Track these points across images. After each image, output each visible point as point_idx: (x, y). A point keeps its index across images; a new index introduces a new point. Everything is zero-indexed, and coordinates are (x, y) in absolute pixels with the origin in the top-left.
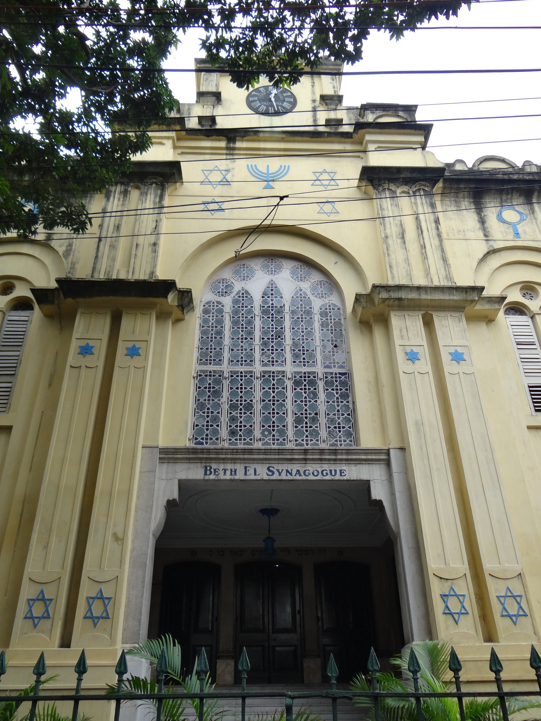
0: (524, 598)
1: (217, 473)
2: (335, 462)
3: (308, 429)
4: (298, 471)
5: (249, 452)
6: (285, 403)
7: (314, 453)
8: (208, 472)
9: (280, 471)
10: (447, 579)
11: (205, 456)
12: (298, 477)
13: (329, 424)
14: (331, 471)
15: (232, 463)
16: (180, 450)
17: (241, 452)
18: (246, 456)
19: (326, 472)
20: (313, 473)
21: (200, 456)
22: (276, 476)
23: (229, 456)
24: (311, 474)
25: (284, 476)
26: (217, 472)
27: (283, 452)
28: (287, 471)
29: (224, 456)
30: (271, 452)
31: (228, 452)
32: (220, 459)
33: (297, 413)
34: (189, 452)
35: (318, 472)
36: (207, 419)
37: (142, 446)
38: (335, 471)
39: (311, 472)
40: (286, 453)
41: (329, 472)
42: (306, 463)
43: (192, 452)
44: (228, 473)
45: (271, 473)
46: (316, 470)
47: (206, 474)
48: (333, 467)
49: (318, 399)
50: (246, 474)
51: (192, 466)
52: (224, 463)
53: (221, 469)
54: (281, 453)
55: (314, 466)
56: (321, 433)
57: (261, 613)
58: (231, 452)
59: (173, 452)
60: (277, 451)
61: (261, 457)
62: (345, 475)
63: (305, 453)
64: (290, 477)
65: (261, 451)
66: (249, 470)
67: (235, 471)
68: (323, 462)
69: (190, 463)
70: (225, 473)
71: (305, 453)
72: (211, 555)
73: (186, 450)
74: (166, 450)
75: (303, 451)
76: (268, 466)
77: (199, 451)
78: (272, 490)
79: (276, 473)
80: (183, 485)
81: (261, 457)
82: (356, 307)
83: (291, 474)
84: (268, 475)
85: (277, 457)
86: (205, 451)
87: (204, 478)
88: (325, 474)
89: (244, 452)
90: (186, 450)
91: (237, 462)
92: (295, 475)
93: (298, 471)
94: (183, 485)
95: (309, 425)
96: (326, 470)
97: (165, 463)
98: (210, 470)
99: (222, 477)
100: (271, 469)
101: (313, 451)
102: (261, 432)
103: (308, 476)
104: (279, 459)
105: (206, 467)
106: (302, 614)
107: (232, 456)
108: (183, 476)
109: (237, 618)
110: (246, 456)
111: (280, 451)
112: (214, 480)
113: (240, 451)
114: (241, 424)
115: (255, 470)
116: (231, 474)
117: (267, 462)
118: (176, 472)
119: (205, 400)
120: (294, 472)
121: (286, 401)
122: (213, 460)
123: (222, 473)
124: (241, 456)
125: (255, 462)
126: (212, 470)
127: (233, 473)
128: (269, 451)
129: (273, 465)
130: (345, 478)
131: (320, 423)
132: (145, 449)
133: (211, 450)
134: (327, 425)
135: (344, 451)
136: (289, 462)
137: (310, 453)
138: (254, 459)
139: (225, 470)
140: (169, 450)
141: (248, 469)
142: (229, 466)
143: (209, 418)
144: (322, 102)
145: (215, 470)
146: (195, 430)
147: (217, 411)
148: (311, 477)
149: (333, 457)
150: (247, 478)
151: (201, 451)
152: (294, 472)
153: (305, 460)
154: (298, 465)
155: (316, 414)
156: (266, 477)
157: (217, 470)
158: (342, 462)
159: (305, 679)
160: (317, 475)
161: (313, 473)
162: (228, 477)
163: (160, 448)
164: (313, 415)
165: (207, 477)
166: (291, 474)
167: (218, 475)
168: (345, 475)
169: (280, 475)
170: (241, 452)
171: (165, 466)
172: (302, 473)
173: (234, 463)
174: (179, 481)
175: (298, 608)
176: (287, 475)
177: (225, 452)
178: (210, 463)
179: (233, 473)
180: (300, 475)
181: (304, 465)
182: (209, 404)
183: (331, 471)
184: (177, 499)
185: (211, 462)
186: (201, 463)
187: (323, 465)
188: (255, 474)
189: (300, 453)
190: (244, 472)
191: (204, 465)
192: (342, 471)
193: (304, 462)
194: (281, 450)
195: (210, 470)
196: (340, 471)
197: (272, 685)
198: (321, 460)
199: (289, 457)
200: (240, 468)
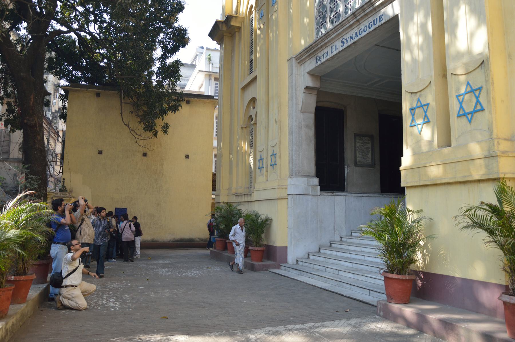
0: (484, 91)
4: (356, 33)
7: (360, 12)
10: (416, 93)
14: (374, 21)
17: (325, 38)
18: (329, 39)
21: (311, 52)
28: (351, 37)
30: (338, 28)
35: (366, 26)
38: (377, 19)
42: (360, 24)
54: (343, 25)
55: (364, 23)
61: (335, 34)
63: (355, 16)
64: (352, 41)
71: (355, 16)
73: (304, 52)
75: (353, 16)
80: (311, 74)
85: (342, 29)
89: (326, 37)
90: (304, 52)
91: (328, 45)
94: (311, 74)
100: (343, 40)
108: (308, 70)
111: (342, 24)
122: (318, 51)
124: (327, 41)
125: (335, 40)
126: (319, 58)
129: (343, 38)
137: (357, 14)
138: (333, 38)
141: (333, 47)
149: (371, 8)
153: (358, 21)
168: (382, 20)
174: (308, 73)
177: (319, 42)
180: (357, 36)
183: (374, 21)
189: (352, 18)
198: (366, 15)
199: (348, 25)
200: (329, 49)
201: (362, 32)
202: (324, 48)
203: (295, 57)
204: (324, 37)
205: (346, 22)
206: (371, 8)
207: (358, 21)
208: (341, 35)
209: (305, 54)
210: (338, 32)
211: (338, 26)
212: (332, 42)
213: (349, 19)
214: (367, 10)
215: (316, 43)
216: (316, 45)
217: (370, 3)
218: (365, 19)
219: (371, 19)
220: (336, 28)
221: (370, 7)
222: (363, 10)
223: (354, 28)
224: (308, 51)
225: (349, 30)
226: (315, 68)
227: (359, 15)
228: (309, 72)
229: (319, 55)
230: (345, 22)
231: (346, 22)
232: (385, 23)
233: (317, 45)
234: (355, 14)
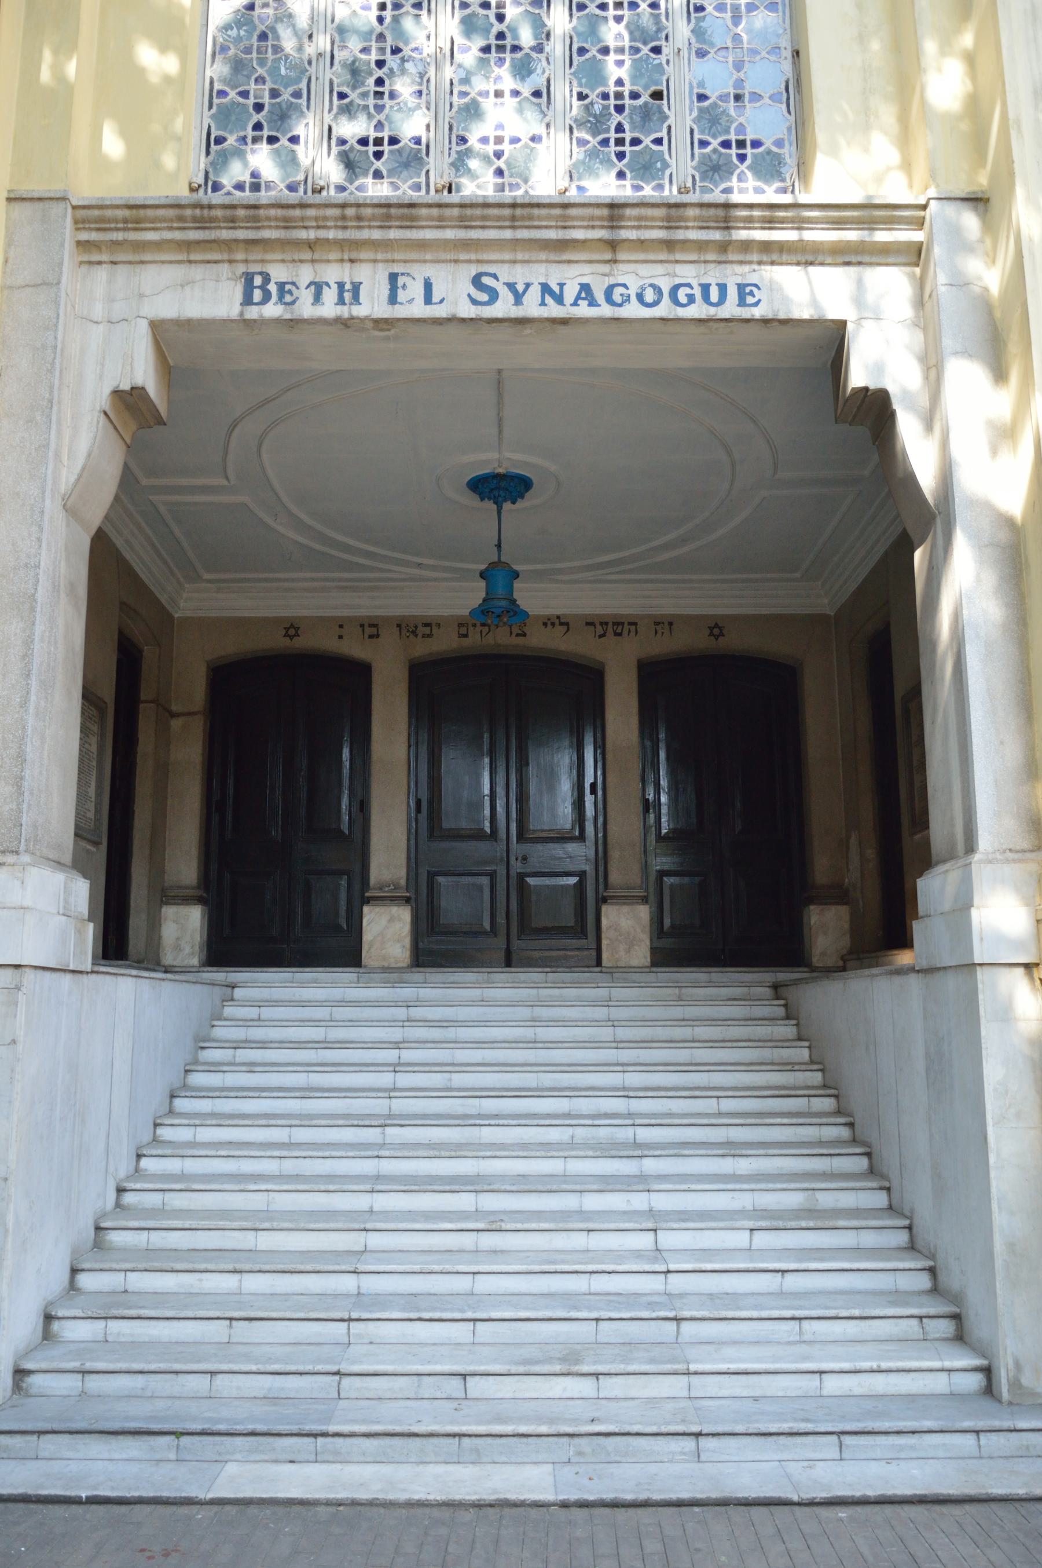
1: (288, 298)
2: (723, 258)
3: (627, 148)
4: (585, 288)
5: (401, 218)
6: (542, 56)
8: (257, 295)
9: (520, 288)
11: (241, 234)
12: (584, 310)
13: (702, 132)
14: (705, 288)
15: (342, 261)
16: (150, 213)
18: (393, 234)
19: (688, 291)
20: (640, 297)
21: (225, 234)
22: (503, 308)
23: (331, 234)
24: (633, 298)
25: (532, 307)
26: (290, 292)
27: (531, 218)
28: (546, 288)
29: (312, 234)
30: (484, 218)
31: (325, 218)
32: (297, 244)
33: (585, 91)
34: (181, 219)
35: (658, 291)
36: (260, 117)
37: (5, 195)
38: (723, 288)
39: (633, 292)
40: (539, 218)
41: (697, 292)
42: (615, 261)
43: (195, 219)
44: (330, 295)
45: (484, 297)
46: (651, 285)
47: (248, 300)
48: (713, 276)
49: (663, 43)
50: (393, 300)
51: (197, 272)
52: (313, 261)
53: (303, 284)
54: (523, 218)
55: (645, 270)
56: (673, 162)
57: (486, 791)
58: (336, 219)
59: (125, 221)
60: (507, 212)
61: (450, 234)
62: (757, 304)
64: (554, 310)
65: (447, 212)
66: (404, 287)
67: (356, 288)
68: (679, 256)
69: (190, 262)
70: (317, 298)
71: (611, 218)
72: (340, 637)
74: (96, 213)
76: (474, 270)
77: (219, 213)
78: (500, 371)
79: (506, 296)
81: (450, 234)
83: (559, 299)
84: (474, 302)
85: (508, 234)
86: (241, 213)
87: (242, 314)
88: (682, 298)
89: (388, 217)
90: (171, 213)
91: (363, 255)
92: (575, 304)
93: (585, 288)
95: (628, 136)
96: (689, 285)
97: (100, 263)
98: (263, 288)
99: (306, 309)
100: (486, 280)
101: (643, 211)
102: (451, 160)
103: (620, 305)
104: (515, 243)
105: (249, 278)
106: (600, 793)
107: (340, 235)
108: (167, 308)
109: (419, 802)
110: (393, 234)
111: (519, 212)
112: (278, 321)
113: (368, 211)
114: (380, 135)
115: (428, 286)
116: (341, 301)
117: (473, 257)
118: (141, 296)
119: (248, 50)
120: (570, 293)
121: (547, 49)
123: (306, 296)
124: (376, 235)
125: (428, 257)
126: (272, 288)
127: (347, 296)
128: (478, 212)
130: (757, 313)
131: (669, 127)
132: (17, 207)
133: (262, 212)
134: (697, 136)
135: (756, 213)
136: (553, 257)
137: (630, 219)
138: (422, 245)
139: (318, 288)
140: (109, 213)
141: (401, 281)
142: (333, 273)
143: (264, 113)
145: (281, 286)
146: (211, 157)
147: (291, 90)
148: (633, 310)
149: (717, 235)
150: (400, 312)
151: (229, 212)
152: (570, 293)
154: (587, 269)
155: (657, 95)
156: (466, 310)
157: (288, 287)
158: (748, 258)
159: (605, 956)
160: (655, 304)
161: (640, 297)
162: (329, 308)
163: (75, 202)
164: (645, 98)
165: (253, 313)
166: (559, 299)
167: (293, 302)
168: (757, 304)
169: (518, 298)
170: (373, 218)
171: (102, 274)
172: (600, 296)
173: (352, 261)
174: (157, 327)
175: (589, 779)
176: (543, 303)
177: (316, 219)
178: (263, 261)
179: (347, 296)
180: (593, 303)
181: (605, 268)
182: (262, 62)
183: (705, 288)
184: (152, 391)
185: (269, 256)
186: (230, 262)
187: (679, 269)
188: (428, 300)
189: (592, 218)
190: (386, 292)
191: (241, 268)
192: (748, 289)
193: (608, 256)
194: (523, 206)
195: (263, 288)
196: (741, 287)
197: (513, 970)
198: (669, 245)
199: (552, 234)
201: (628, 299)
202: (333, 256)
203: (74, 207)
204: (368, 211)
205: (549, 218)
206: (717, 235)
207: (613, 245)
208: (476, 251)
209: (171, 229)
210: (474, 234)
212: (396, 256)
213: (573, 212)
214: (687, 228)
215: (292, 213)
216: (286, 219)
217: (721, 212)
218: (652, 257)
219: (688, 273)
221: (708, 228)
222: (669, 219)
223: (569, 262)
224: (202, 223)
225: (543, 256)
226: (172, 320)
227: (639, 227)
228: (163, 321)
229: (278, 273)
230: (544, 212)
231: (549, 218)
232: (765, 322)
233: (287, 224)
234: (616, 211)
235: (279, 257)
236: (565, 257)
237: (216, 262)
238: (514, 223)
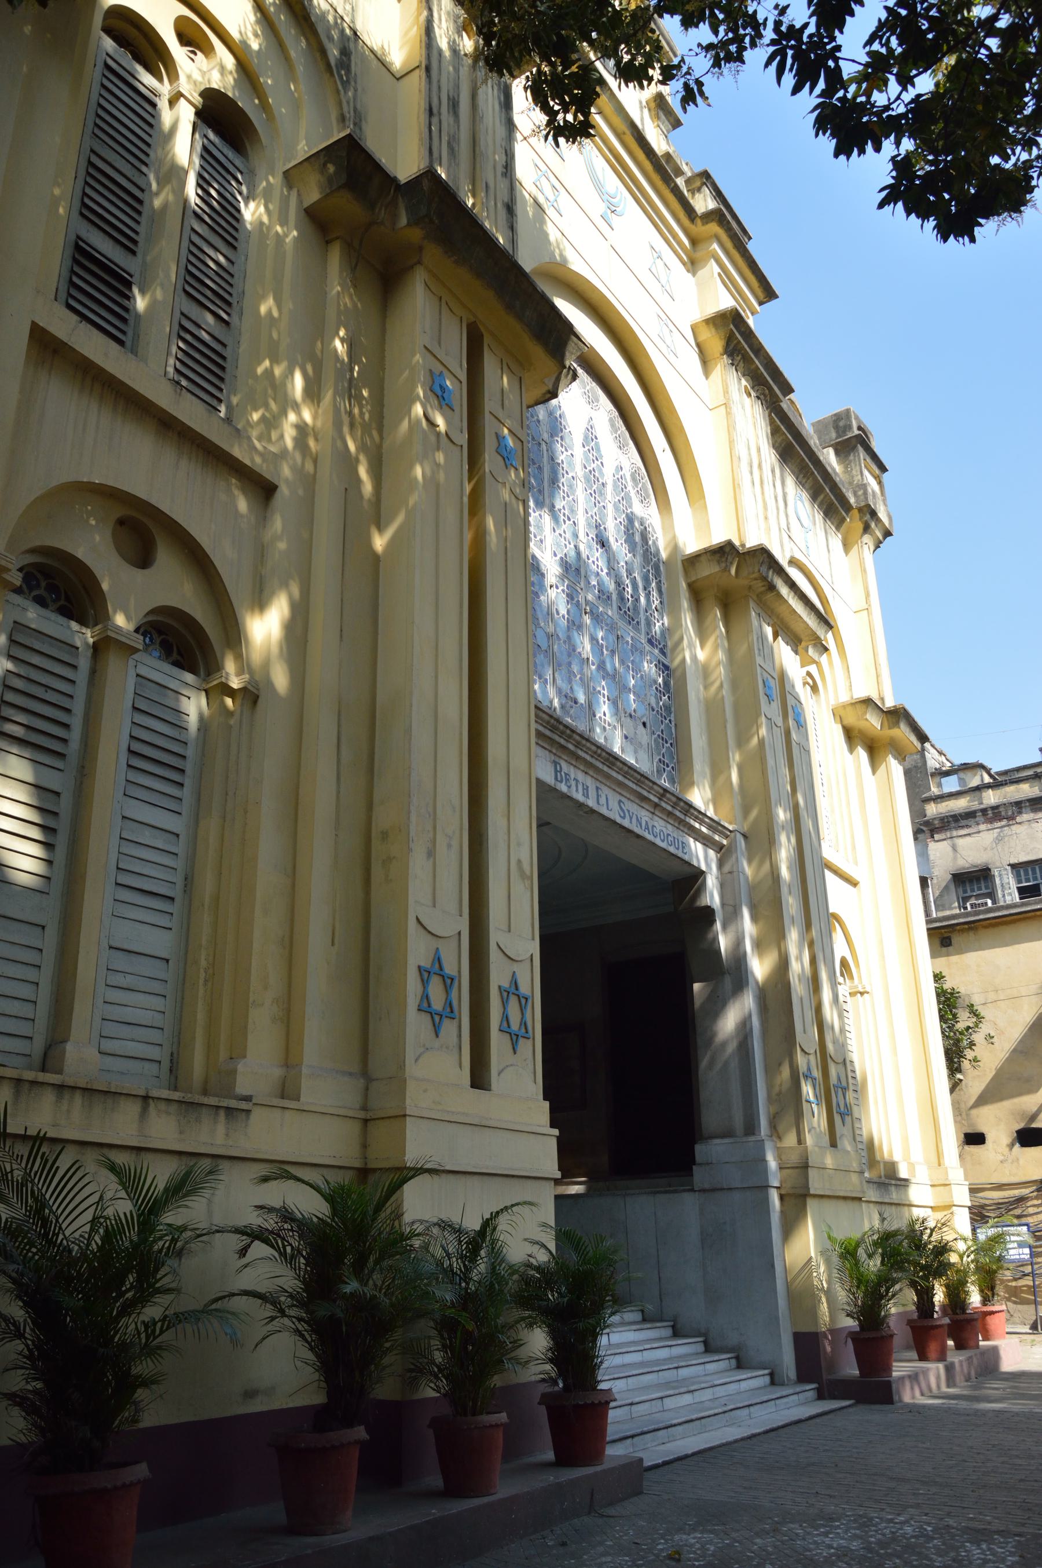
68: (670, 821)
82: (703, 559)
89: (607, 760)
111: (642, 779)
138: (608, 777)
144: (653, 105)
205: (647, 786)
211: (636, 775)
213: (655, 787)
215: (584, 742)
220: (632, 772)
224: (553, 729)
231: (647, 786)
235: (566, 758)
236: (642, 805)
237: (545, 749)
238: (638, 783)
